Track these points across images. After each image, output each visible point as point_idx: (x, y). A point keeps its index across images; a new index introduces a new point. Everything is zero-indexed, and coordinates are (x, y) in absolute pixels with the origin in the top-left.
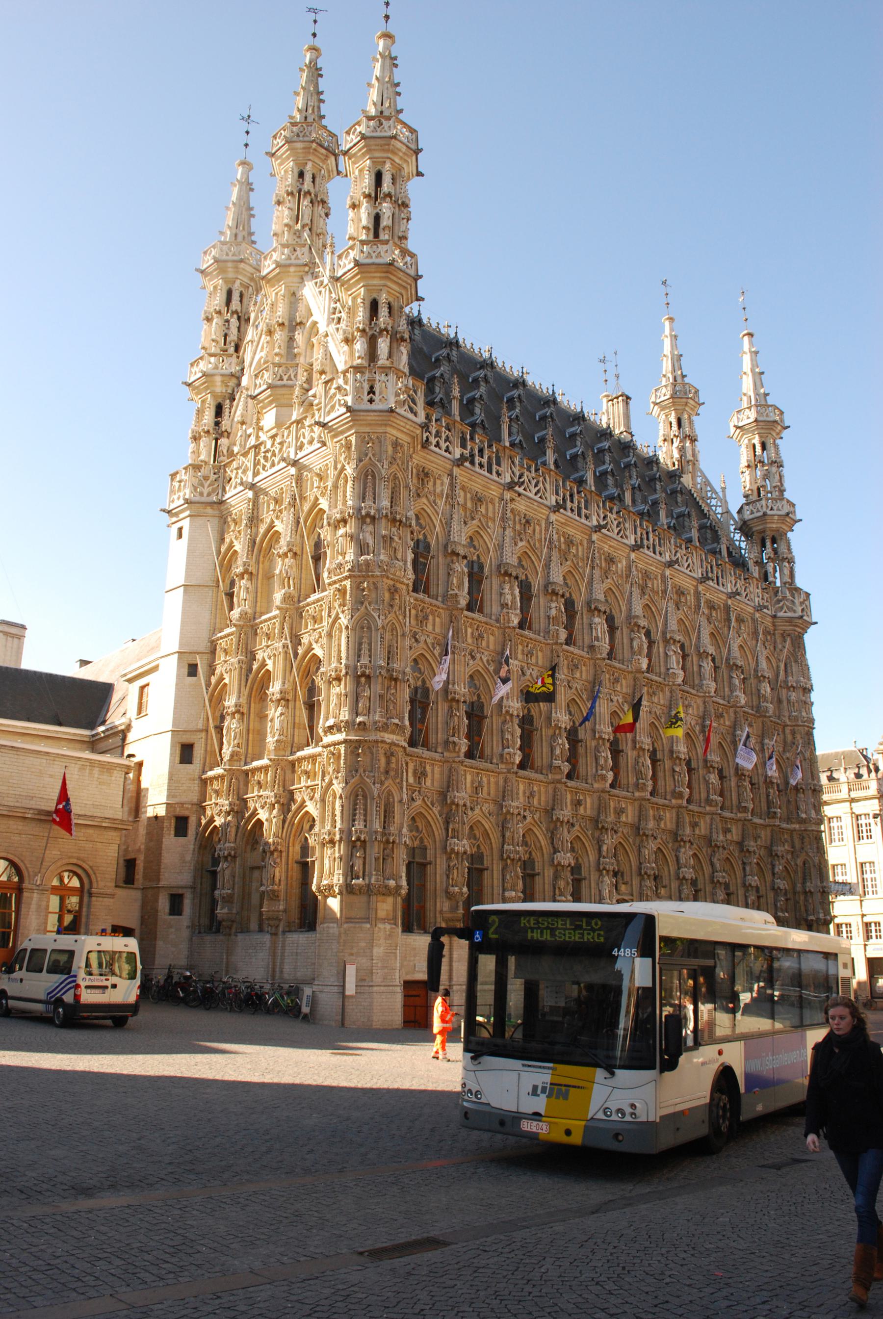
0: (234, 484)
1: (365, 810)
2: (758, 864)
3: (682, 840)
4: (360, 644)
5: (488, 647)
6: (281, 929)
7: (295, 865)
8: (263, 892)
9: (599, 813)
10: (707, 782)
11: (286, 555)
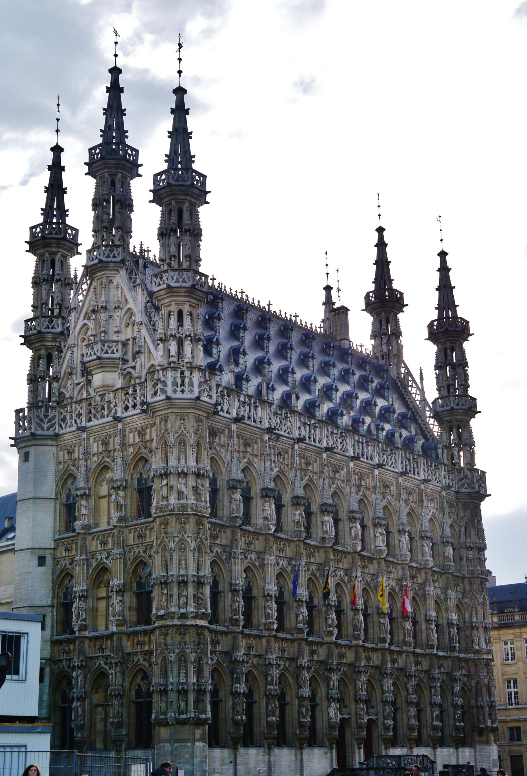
0: (69, 423)
1: (186, 670)
3: (385, 673)
4: (180, 560)
5: (255, 548)
7: (133, 705)
10: (404, 628)
11: (118, 488)
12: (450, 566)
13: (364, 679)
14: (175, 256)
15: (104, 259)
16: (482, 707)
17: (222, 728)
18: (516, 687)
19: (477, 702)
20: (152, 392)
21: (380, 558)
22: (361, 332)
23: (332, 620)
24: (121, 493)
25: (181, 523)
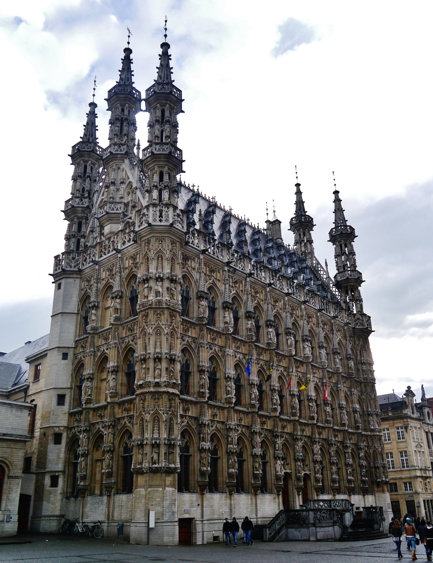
0: (88, 261)
1: (159, 427)
2: (351, 453)
3: (315, 441)
4: (156, 342)
6: (113, 493)
7: (120, 458)
8: (104, 473)
9: (274, 427)
10: (325, 411)
12: (352, 373)
13: (300, 444)
14: (158, 137)
15: (114, 152)
16: (378, 467)
17: (191, 477)
18: (392, 457)
19: (374, 464)
20: (139, 224)
21: (308, 362)
22: (288, 238)
23: (276, 400)
24: (118, 301)
25: (157, 315)
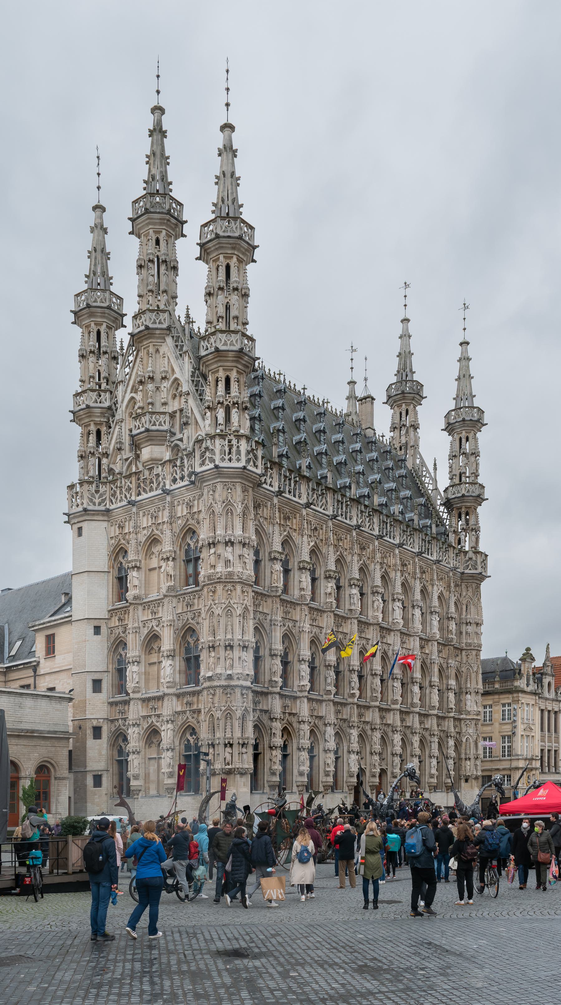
24: (171, 563)
